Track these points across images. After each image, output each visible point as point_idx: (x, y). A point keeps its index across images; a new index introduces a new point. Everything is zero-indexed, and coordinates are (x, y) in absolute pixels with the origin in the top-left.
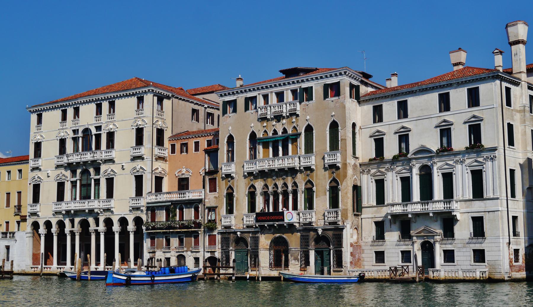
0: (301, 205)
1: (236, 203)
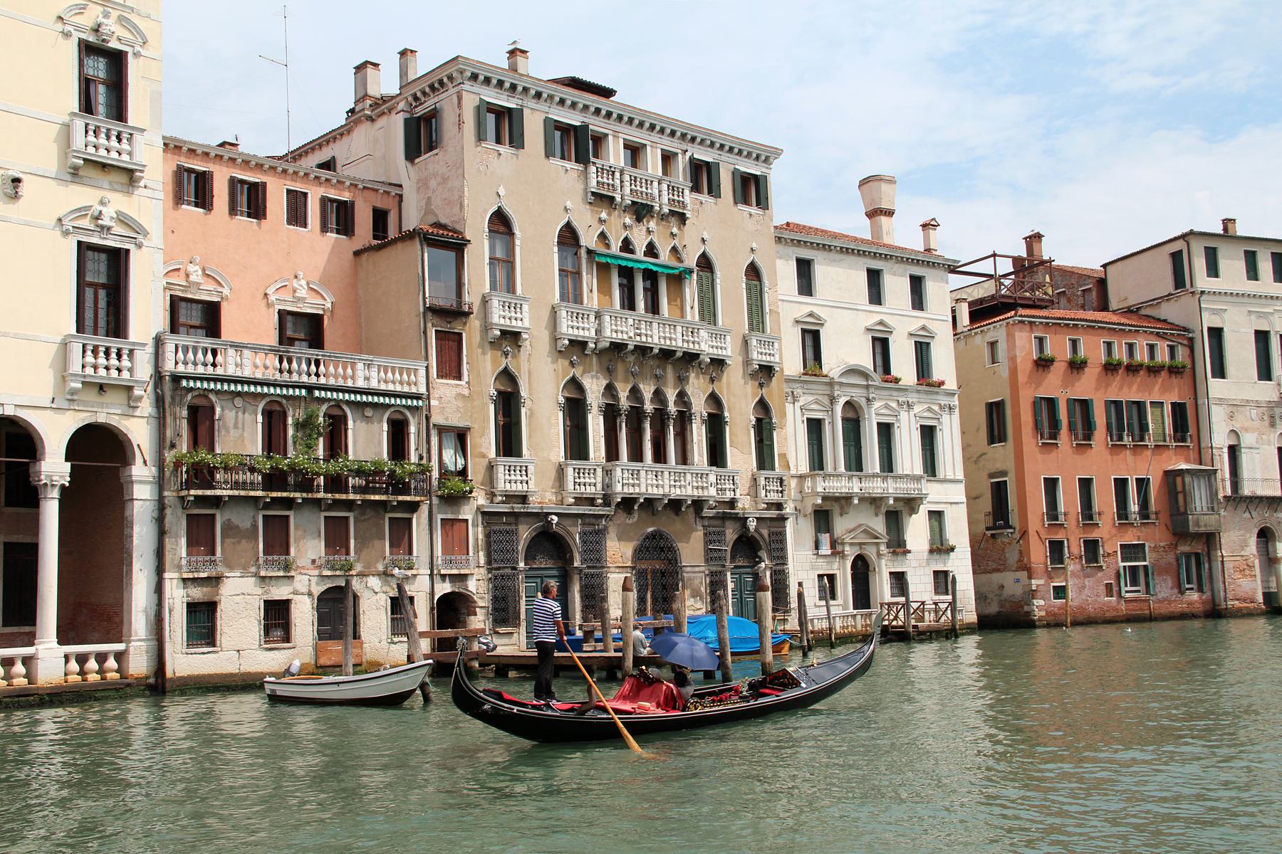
0: (701, 455)
1: (529, 425)
